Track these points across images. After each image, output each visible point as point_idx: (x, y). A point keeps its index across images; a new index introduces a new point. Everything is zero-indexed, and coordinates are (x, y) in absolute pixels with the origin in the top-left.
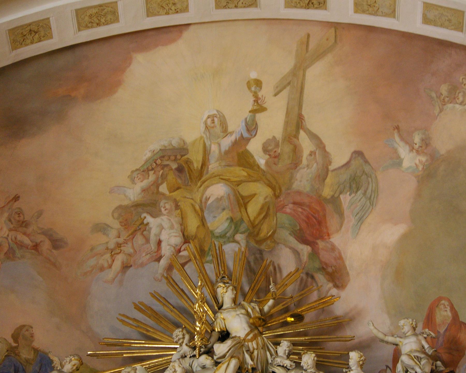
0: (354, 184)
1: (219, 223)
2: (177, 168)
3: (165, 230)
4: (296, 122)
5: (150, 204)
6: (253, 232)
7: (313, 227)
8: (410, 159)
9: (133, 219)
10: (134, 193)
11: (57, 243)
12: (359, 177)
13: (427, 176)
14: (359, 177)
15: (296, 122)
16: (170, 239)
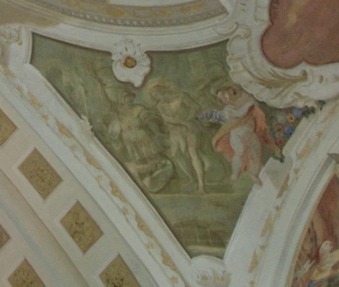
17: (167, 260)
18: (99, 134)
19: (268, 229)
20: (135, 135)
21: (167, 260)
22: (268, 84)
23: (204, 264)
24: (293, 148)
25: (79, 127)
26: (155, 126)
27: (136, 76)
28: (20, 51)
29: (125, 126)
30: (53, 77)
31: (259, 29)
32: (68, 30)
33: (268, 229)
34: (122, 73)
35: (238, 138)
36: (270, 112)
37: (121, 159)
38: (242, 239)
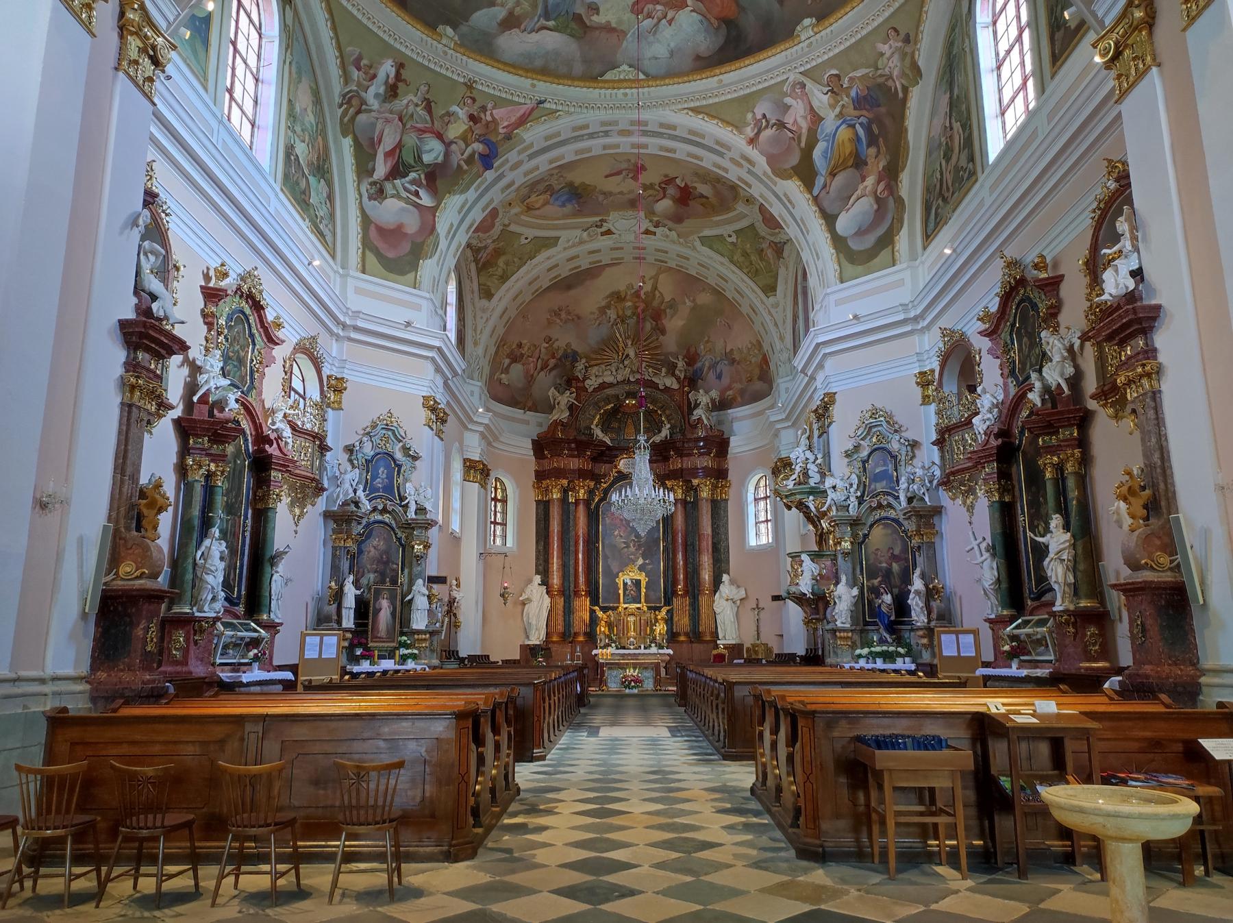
0: (671, 307)
1: (629, 313)
2: (617, 297)
3: (612, 314)
4: (655, 288)
5: (608, 306)
6: (638, 317)
7: (657, 316)
8: (688, 303)
9: (602, 311)
10: (603, 304)
11: (579, 318)
12: (673, 305)
13: (693, 309)
14: (673, 305)
15: (655, 288)
16: (613, 316)
17: (763, 302)
18: (732, 261)
19: (786, 283)
20: (741, 259)
21: (763, 302)
22: (771, 235)
23: (772, 299)
24: (785, 254)
25: (725, 260)
26: (745, 254)
27: (733, 239)
28: (698, 243)
29: (737, 257)
30: (711, 248)
31: (761, 218)
32: (707, 232)
33: (786, 283)
34: (730, 240)
35: (770, 253)
36: (776, 244)
37: (740, 268)
38: (780, 288)
